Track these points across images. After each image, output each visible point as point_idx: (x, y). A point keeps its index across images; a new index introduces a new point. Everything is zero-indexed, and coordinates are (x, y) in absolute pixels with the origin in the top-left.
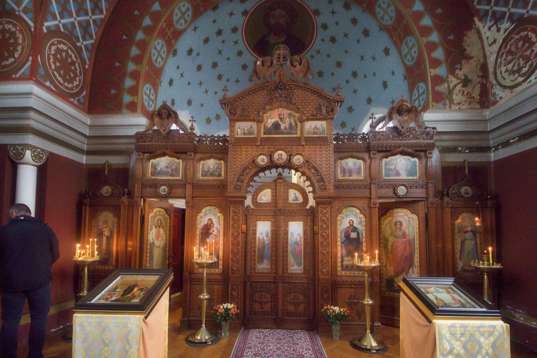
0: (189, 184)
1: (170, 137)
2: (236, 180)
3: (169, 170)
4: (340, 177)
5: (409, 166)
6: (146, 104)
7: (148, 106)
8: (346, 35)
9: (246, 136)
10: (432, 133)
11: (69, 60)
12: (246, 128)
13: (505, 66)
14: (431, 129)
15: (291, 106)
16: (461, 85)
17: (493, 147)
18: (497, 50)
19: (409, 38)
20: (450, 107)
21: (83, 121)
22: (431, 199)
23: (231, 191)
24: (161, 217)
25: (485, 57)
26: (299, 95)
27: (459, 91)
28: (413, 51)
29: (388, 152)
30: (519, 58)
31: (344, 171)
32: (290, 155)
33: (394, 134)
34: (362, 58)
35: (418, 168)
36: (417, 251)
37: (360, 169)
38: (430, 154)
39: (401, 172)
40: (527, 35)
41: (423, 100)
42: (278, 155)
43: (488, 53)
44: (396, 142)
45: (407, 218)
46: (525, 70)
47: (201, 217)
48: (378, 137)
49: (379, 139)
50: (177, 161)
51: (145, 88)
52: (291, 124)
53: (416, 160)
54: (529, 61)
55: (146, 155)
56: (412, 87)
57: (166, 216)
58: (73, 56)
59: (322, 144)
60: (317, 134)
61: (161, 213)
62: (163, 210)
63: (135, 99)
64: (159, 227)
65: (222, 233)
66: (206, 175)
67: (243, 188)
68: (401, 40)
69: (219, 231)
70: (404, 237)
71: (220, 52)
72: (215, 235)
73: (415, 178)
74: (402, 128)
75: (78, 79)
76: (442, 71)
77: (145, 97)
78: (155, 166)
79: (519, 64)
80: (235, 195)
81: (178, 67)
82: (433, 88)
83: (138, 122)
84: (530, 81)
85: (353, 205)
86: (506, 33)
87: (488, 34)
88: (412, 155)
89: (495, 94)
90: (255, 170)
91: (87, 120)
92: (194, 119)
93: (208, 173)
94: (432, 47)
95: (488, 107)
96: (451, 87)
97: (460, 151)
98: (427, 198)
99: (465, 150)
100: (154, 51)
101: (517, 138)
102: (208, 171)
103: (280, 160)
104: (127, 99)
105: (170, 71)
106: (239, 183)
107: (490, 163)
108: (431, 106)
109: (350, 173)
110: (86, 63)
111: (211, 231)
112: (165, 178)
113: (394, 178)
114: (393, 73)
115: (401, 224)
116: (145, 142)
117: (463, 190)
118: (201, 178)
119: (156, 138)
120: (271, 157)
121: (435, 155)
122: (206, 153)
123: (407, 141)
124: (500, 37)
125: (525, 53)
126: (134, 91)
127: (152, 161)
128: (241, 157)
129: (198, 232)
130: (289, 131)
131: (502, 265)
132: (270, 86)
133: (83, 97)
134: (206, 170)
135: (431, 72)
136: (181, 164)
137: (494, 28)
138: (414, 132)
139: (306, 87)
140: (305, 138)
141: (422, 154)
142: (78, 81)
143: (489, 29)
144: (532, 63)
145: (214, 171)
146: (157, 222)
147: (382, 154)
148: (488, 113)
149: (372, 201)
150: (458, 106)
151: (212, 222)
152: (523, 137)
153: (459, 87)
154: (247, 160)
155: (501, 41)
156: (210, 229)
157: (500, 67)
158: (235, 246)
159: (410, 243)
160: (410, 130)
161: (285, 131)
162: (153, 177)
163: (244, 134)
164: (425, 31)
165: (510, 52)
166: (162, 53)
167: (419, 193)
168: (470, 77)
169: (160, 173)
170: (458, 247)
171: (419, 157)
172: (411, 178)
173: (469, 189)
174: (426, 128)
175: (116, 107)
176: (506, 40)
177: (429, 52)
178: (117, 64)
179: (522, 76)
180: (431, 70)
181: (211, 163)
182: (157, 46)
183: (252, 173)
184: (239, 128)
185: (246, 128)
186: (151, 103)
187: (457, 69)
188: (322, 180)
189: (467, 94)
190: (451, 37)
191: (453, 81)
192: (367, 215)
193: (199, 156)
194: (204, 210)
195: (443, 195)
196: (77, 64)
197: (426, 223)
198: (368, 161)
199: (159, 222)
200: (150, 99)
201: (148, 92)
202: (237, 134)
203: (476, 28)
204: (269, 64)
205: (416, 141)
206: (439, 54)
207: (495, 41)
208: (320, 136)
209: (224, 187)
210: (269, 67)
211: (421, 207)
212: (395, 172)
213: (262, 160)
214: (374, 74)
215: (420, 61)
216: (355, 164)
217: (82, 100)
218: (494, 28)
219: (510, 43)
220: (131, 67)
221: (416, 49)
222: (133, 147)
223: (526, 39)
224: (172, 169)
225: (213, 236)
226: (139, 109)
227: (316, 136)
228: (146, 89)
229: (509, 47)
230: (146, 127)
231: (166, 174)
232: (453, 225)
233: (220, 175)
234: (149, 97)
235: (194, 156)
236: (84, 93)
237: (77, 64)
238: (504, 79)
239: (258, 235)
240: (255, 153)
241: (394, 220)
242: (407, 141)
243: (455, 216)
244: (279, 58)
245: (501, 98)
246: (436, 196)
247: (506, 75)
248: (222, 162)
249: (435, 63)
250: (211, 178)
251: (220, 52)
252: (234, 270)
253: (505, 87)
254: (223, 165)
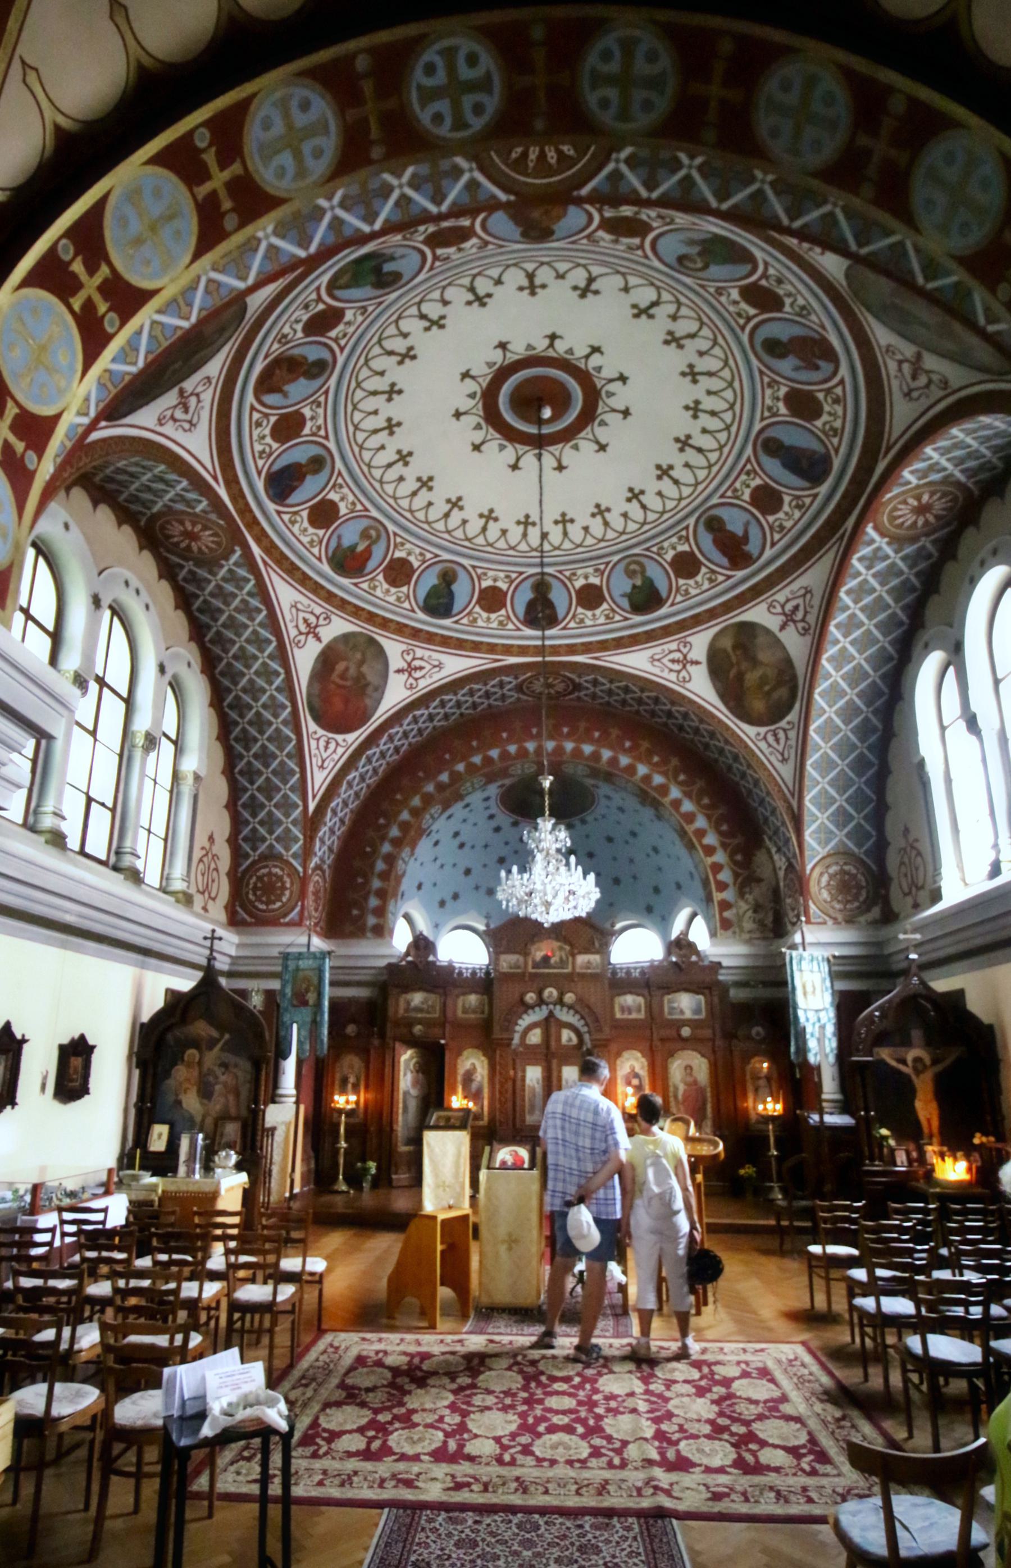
23: (497, 1034)
29: (671, 988)
31: (623, 1009)
76: (728, 895)
88: (696, 992)
109: (630, 1011)
120: (540, 993)
153: (750, 913)
164: (710, 851)
177: (715, 874)
188: (597, 1020)
191: (743, 906)
206: (725, 876)
239: (528, 1081)
249: (722, 886)
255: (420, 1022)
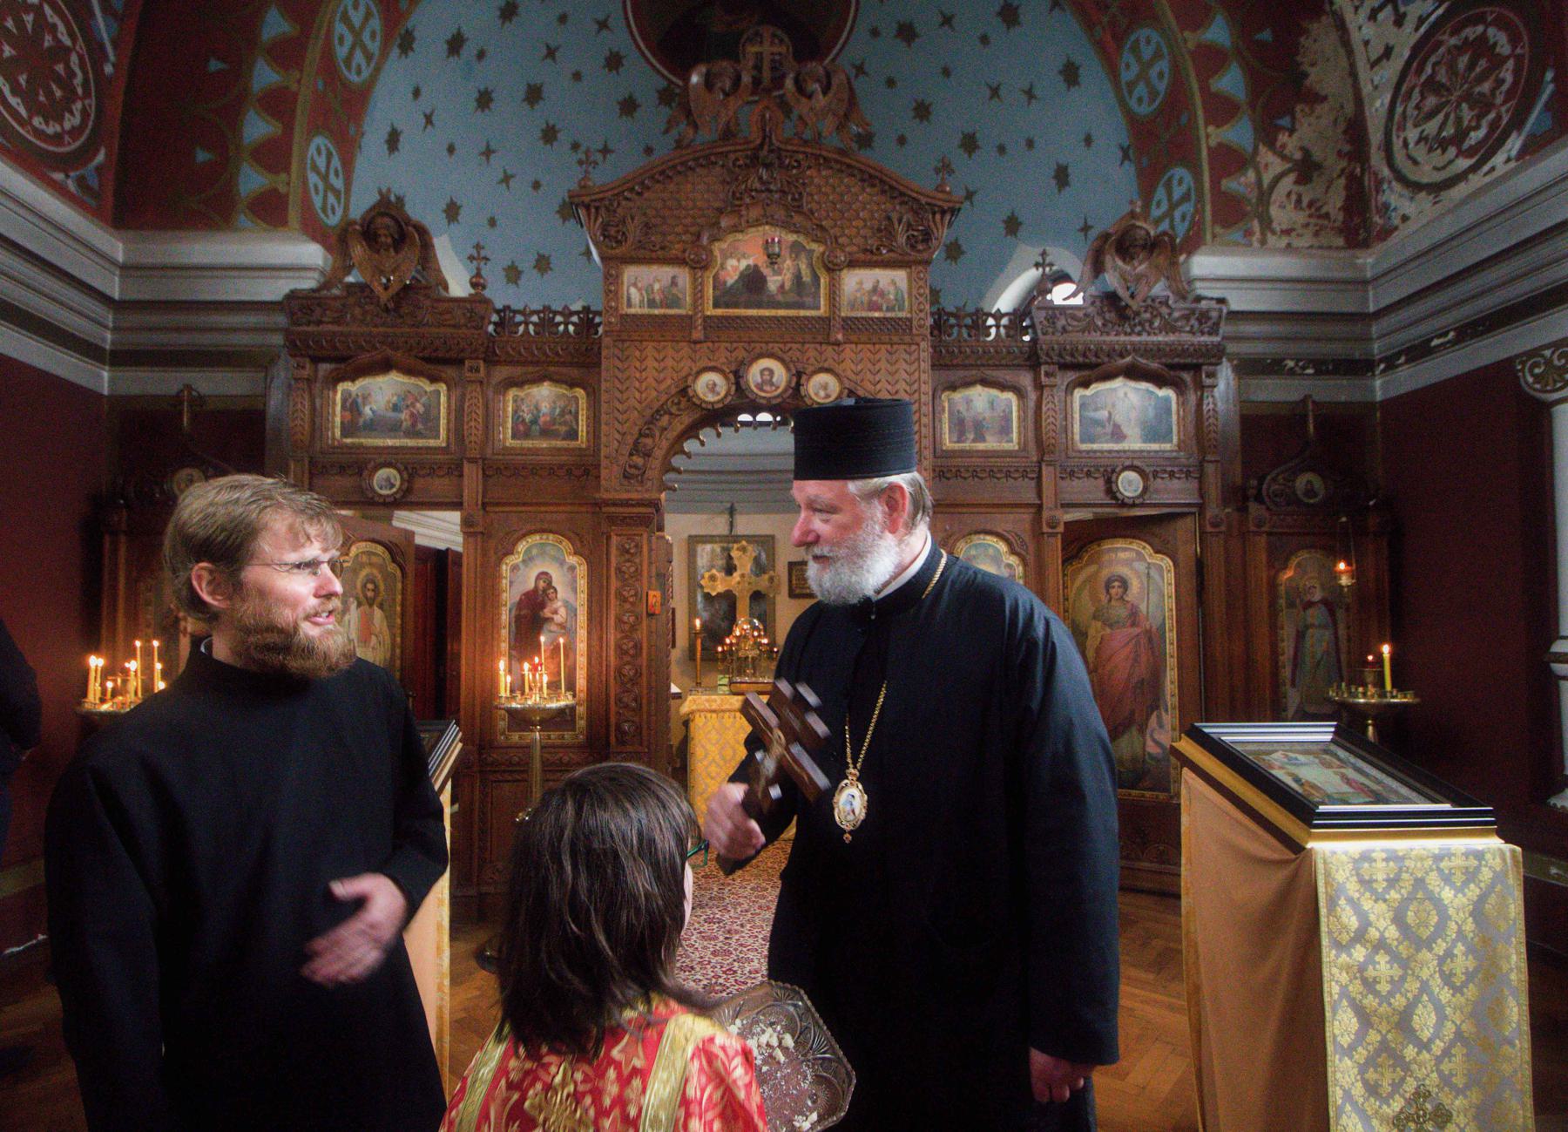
0: (472, 461)
1: (405, 310)
2: (626, 450)
3: (404, 416)
4: (948, 443)
5: (1151, 413)
6: (317, 201)
7: (324, 209)
8: (947, 21)
9: (656, 312)
10: (1214, 314)
11: (48, 41)
12: (657, 287)
13: (1416, 126)
14: (1213, 304)
15: (797, 219)
16: (1292, 177)
17: (1381, 361)
18: (1395, 80)
19: (1143, 33)
20: (1263, 242)
21: (102, 250)
22: (1213, 511)
23: (611, 485)
24: (375, 571)
25: (1359, 101)
26: (821, 185)
27: (1289, 194)
28: (1153, 72)
29: (1092, 368)
30: (1458, 106)
31: (960, 426)
32: (799, 375)
33: (1107, 316)
34: (995, 92)
35: (1174, 417)
36: (1171, 662)
37: (1007, 419)
38: (1208, 376)
39: (1125, 430)
40: (1483, 38)
41: (1183, 218)
42: (762, 372)
43: (1367, 89)
44: (1112, 338)
45: (1141, 566)
46: (1476, 136)
47: (515, 568)
48: (1061, 322)
49: (1064, 330)
50: (429, 387)
51: (312, 150)
52: (798, 277)
53: (1168, 393)
54: (1488, 112)
55: (325, 368)
56: (1149, 180)
57: (392, 568)
58: (61, 28)
59: (895, 339)
60: (879, 309)
61: (374, 559)
62: (380, 549)
63: (280, 182)
64: (371, 605)
65: (582, 618)
66: (527, 435)
67: (649, 473)
68: (1119, 39)
69: (573, 612)
70: (1133, 625)
71: (551, 53)
72: (562, 626)
73: (1167, 446)
74: (1132, 296)
75: (77, 107)
76: (1239, 133)
77: (313, 179)
78: (355, 403)
79: (1459, 120)
80: (625, 496)
81: (417, 93)
82: (1215, 183)
83: (296, 259)
84: (1493, 169)
85: (988, 527)
86: (1422, 30)
87: (1369, 31)
88: (1159, 380)
89: (1386, 206)
90: (686, 420)
91: (117, 247)
92: (483, 253)
93: (535, 428)
94: (1211, 59)
95: (1365, 244)
96: (1267, 179)
97: (1291, 372)
98: (1201, 507)
99: (1304, 368)
100: (340, 28)
101: (1452, 334)
102: (535, 421)
103: (767, 388)
104: (252, 180)
105: (389, 105)
106: (639, 461)
107: (1371, 406)
108: (1209, 237)
110: (105, 58)
111: (547, 613)
112: (390, 442)
113: (1106, 446)
114: (1088, 141)
115: (1124, 584)
116: (320, 323)
117: (1301, 482)
118: (510, 442)
119: (357, 311)
120: (737, 377)
121: (1224, 381)
122: (525, 363)
123: (1144, 338)
124: (1406, 40)
125: (1477, 89)
126: (274, 156)
127: (341, 387)
128: (645, 376)
129: (505, 617)
130: (792, 297)
131: (1416, 695)
132: (732, 156)
133: (99, 169)
134: (528, 417)
135: (1211, 136)
136: (443, 399)
137: (1386, 14)
138: (1164, 310)
139: (842, 163)
140: (845, 319)
141: (1187, 377)
142: (78, 114)
143: (1373, 15)
144: (1499, 117)
145: (553, 422)
146: (364, 586)
147: (1071, 376)
148: (1370, 260)
149: (1045, 514)
150: (1284, 241)
151: (549, 585)
152: (1470, 331)
153: (1287, 183)
154: (663, 386)
155: (1407, 54)
156: (542, 606)
157: (1402, 128)
158: (627, 658)
159: (1150, 640)
160: (1153, 305)
161: (780, 298)
162: (349, 441)
163: (652, 303)
165: (1432, 85)
166: (366, 37)
167: (1176, 492)
168: (1317, 155)
169: (373, 426)
170: (1287, 647)
171: (1178, 386)
172: (1155, 447)
173: (1318, 483)
174: (1199, 299)
175: (212, 208)
176: (1421, 50)
178: (214, 65)
179: (1469, 153)
180: (1211, 129)
181: (544, 396)
182: (351, 12)
183: (679, 427)
184: (635, 285)
185: (657, 287)
186: (331, 199)
187: (1282, 128)
189: (1310, 205)
190: (1266, 35)
191: (1272, 164)
192: (1030, 558)
193: (502, 372)
194: (522, 547)
195: (1246, 498)
196: (74, 59)
197: (1197, 582)
198: (1032, 396)
199: (370, 586)
200: (329, 187)
201: (321, 162)
202: (629, 305)
203: (1334, 13)
204: (728, 85)
205: (1172, 338)
206: (1231, 82)
207: (1388, 52)
208: (889, 315)
209: (586, 473)
210: (727, 95)
211: (1184, 531)
212: (1109, 429)
213: (711, 387)
214: (1030, 144)
215: (1175, 101)
216: (992, 403)
217: (94, 183)
218: (1386, 14)
219: (1433, 59)
220: (264, 76)
221: (1163, 65)
222: (278, 339)
223: (1481, 47)
224: (412, 415)
225: (553, 628)
226: (293, 215)
227: (876, 315)
228: (317, 149)
229: (1429, 70)
230: (322, 273)
231: (394, 429)
232: (1273, 585)
233: (572, 434)
234: (325, 178)
235: (488, 374)
236: (101, 157)
237: (74, 59)
238: (1415, 162)
240: (686, 365)
241: (1105, 573)
242: (1144, 338)
243: (1278, 559)
244: (758, 68)
245: (1405, 218)
246: (1225, 502)
247: (1420, 153)
248: (580, 392)
249: (1222, 110)
250: (544, 444)
251: (551, 53)
252: (625, 733)
253: (1416, 187)
254: (583, 403)
255: (390, 458)
